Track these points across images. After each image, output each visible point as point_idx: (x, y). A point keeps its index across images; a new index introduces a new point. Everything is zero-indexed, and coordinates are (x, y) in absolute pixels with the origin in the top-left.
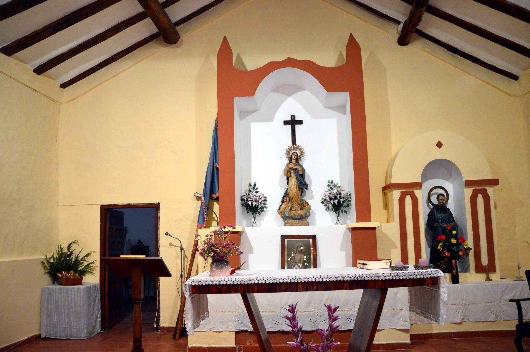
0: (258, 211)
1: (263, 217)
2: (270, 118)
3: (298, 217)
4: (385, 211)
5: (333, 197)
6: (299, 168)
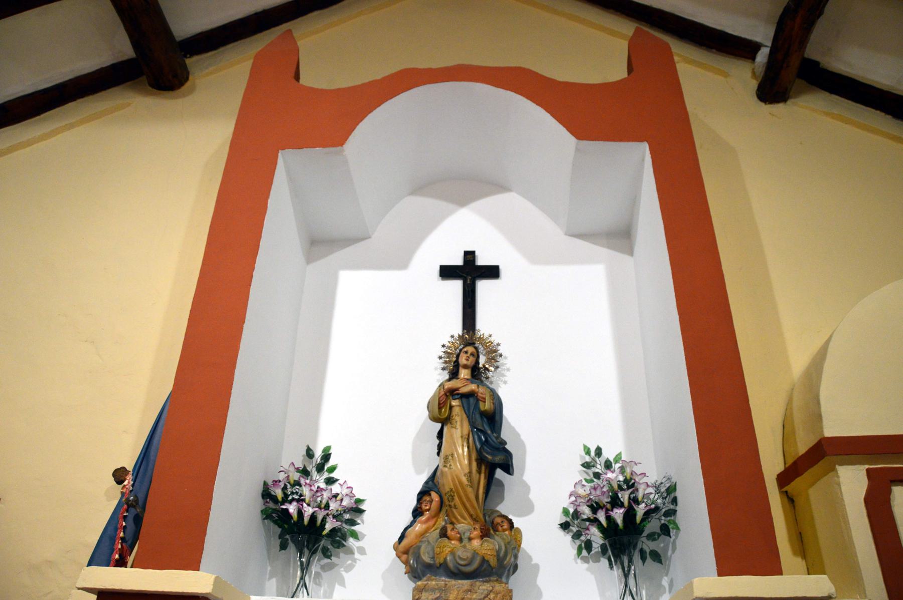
1: (344, 573)
3: (465, 566)
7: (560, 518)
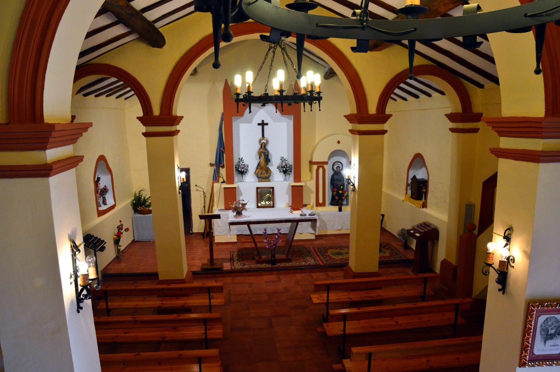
0: (244, 173)
2: (250, 121)
4: (310, 173)
6: (266, 152)
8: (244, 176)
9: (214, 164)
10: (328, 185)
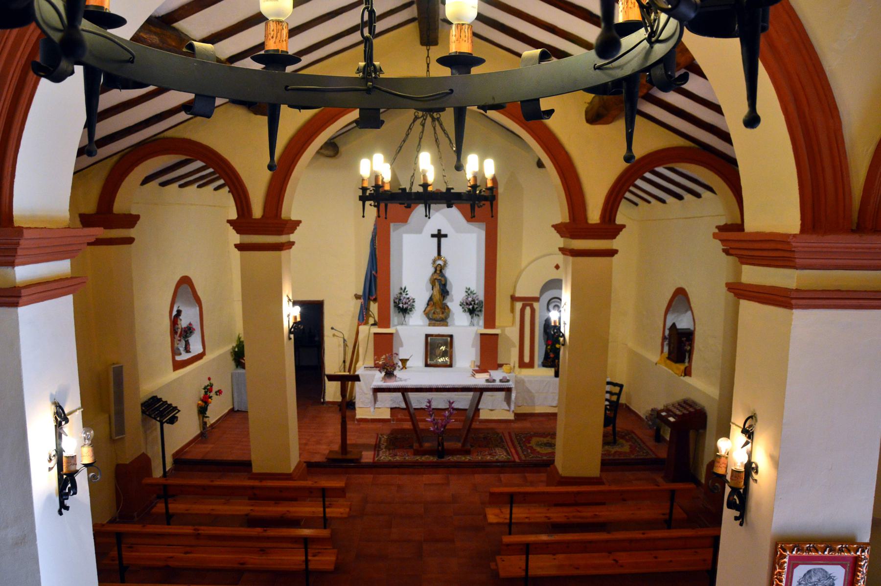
0: (408, 311)
2: (419, 231)
4: (512, 314)
5: (469, 303)
6: (443, 279)
7: (459, 304)
8: (407, 316)
9: (361, 296)
10: (539, 333)
